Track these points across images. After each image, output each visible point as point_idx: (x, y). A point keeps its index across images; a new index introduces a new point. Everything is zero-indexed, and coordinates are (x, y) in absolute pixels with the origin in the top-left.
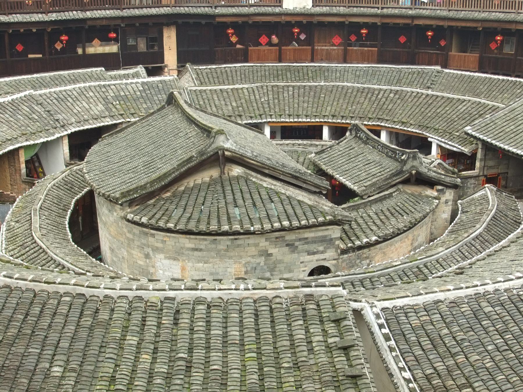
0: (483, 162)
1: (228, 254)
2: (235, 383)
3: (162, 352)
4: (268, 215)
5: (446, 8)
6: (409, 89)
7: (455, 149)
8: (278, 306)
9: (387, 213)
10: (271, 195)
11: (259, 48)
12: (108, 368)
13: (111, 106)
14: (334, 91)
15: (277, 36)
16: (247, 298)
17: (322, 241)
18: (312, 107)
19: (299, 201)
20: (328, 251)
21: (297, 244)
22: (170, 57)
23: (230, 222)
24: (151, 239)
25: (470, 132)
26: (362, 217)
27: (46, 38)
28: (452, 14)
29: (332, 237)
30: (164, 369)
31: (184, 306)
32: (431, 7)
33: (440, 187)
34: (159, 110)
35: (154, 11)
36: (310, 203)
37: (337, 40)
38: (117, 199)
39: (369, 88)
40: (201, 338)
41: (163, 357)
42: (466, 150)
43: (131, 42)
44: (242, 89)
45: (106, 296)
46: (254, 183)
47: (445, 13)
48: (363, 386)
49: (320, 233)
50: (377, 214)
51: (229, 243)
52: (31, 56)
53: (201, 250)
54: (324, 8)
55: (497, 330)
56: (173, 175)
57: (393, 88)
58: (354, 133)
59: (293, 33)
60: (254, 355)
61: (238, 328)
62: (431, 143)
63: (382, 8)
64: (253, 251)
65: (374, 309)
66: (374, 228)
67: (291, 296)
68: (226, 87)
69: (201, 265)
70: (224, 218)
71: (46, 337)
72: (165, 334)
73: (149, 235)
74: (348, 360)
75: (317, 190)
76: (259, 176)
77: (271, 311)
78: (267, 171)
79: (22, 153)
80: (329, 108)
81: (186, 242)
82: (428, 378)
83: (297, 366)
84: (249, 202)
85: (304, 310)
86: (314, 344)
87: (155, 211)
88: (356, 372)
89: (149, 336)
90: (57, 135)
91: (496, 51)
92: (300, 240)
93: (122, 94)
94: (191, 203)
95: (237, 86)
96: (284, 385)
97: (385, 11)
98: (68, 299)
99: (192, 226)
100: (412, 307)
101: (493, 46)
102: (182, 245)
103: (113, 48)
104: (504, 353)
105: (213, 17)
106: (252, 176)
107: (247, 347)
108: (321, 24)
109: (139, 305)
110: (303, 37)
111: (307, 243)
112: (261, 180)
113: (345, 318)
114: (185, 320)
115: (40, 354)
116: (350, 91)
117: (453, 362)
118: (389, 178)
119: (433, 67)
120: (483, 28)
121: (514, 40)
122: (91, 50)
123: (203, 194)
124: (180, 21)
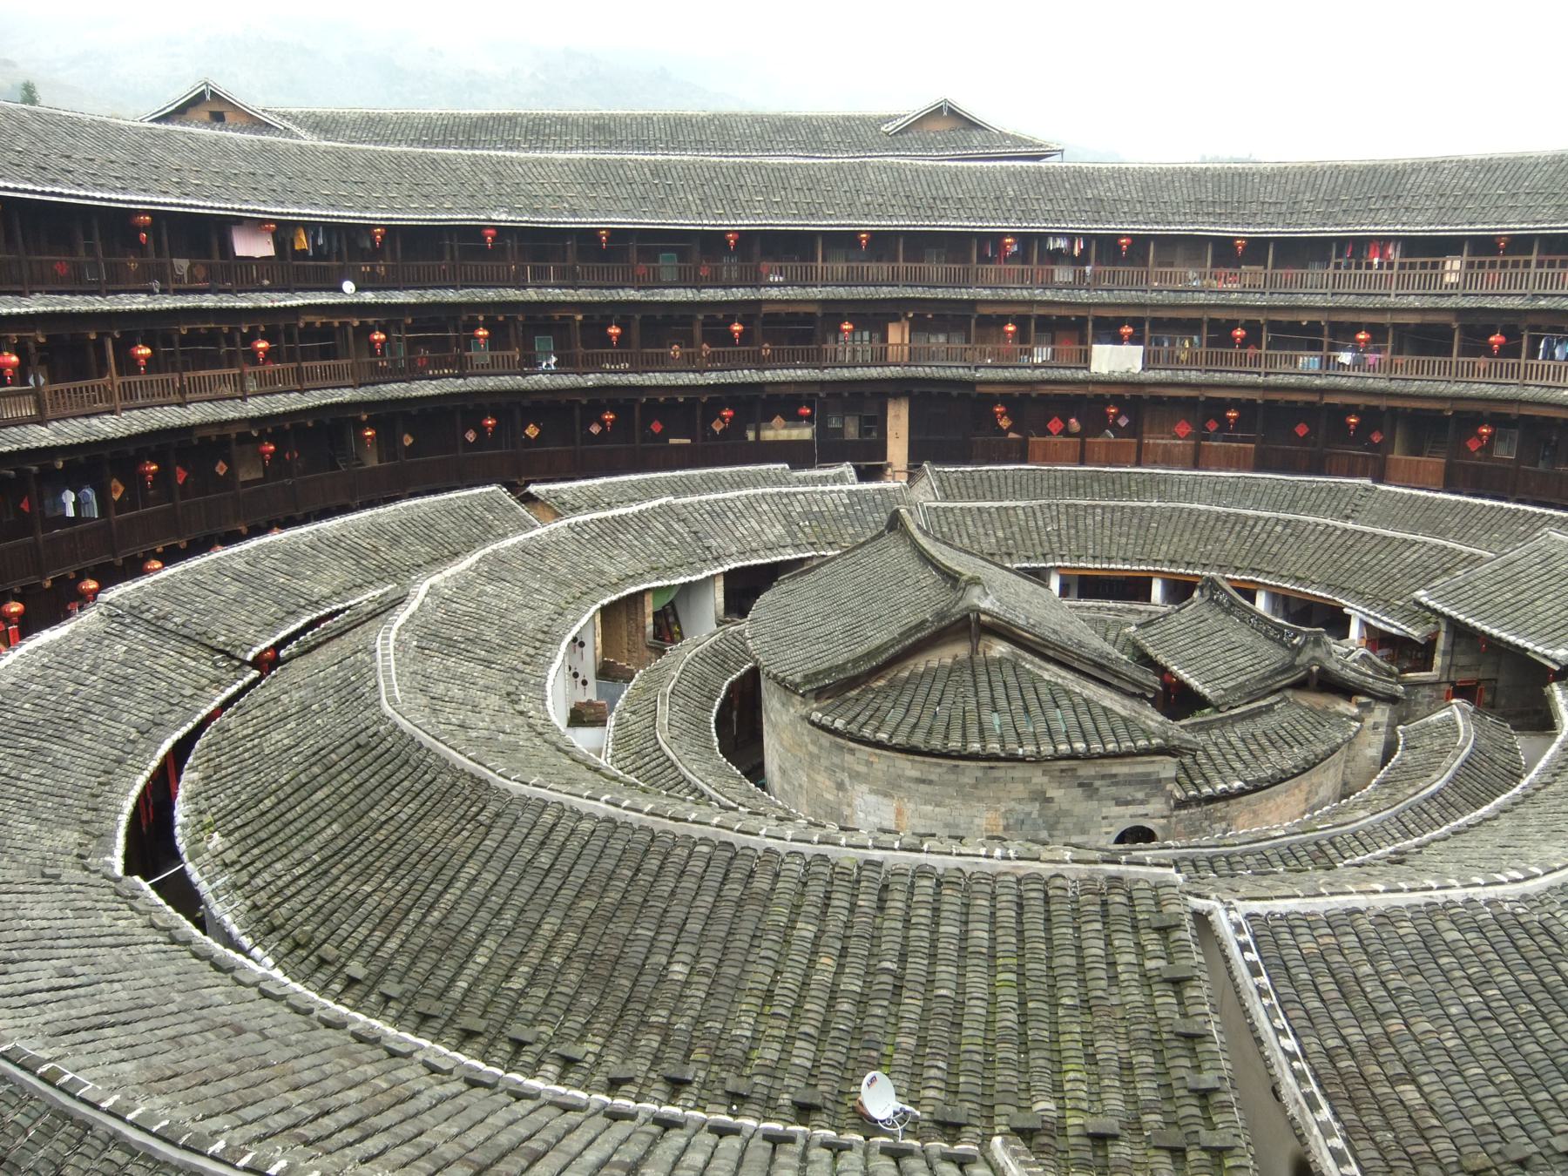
0: (1448, 658)
1: (977, 793)
2: (975, 1025)
3: (855, 955)
4: (1049, 729)
6: (1311, 519)
7: (1394, 631)
8: (1060, 892)
9: (1264, 741)
10: (1057, 695)
11: (1047, 439)
12: (761, 975)
13: (795, 528)
14: (1174, 519)
15: (1078, 419)
16: (1006, 874)
17: (1143, 782)
18: (1135, 545)
19: (1104, 708)
20: (1153, 800)
21: (1097, 783)
22: (897, 450)
23: (983, 739)
24: (848, 757)
25: (1424, 600)
26: (1216, 744)
27: (699, 413)
28: (1394, 386)
29: (1162, 776)
30: (856, 986)
31: (896, 878)
33: (1363, 699)
34: (873, 539)
35: (874, 372)
36: (1124, 713)
37: (1183, 428)
38: (797, 686)
39: (1238, 515)
40: (921, 938)
41: (854, 966)
42: (1416, 633)
43: (834, 423)
44: (1014, 508)
45: (768, 850)
46: (1029, 672)
47: (1382, 384)
48: (1207, 1056)
49: (1140, 767)
50: (1243, 740)
51: (979, 774)
52: (672, 441)
53: (930, 782)
54: (1163, 373)
55: (1469, 978)
56: (892, 651)
57: (1282, 515)
58: (1207, 593)
59: (1107, 415)
60: (1013, 977)
61: (986, 926)
62: (1347, 619)
63: (1267, 374)
64: (1019, 790)
65: (1233, 915)
66: (1238, 765)
67: (1083, 876)
68: (987, 504)
69: (930, 808)
70: (973, 730)
71: (665, 911)
72: (861, 923)
74: (1180, 1003)
75: (1138, 691)
76: (1037, 660)
77: (1047, 900)
78: (1050, 653)
79: (649, 599)
80: (1164, 548)
81: (908, 767)
82: (1330, 1055)
83: (1086, 1005)
84: (1017, 704)
85: (1104, 903)
86: (1120, 968)
87: (857, 709)
88: (1194, 1029)
89: (834, 926)
90: (707, 573)
92: (1103, 777)
93: (815, 509)
94: (919, 699)
95: (1006, 503)
96: (1062, 1038)
97: (1271, 378)
98: (705, 849)
99: (918, 740)
100: (1304, 917)
101: (1473, 445)
103: (805, 433)
104: (1481, 1025)
105: (972, 384)
107: (1000, 961)
108: (1157, 401)
109: (821, 869)
110: (1123, 422)
111: (1116, 784)
112: (1040, 667)
113: (1178, 926)
114: (896, 903)
115: (654, 939)
116: (1203, 518)
117: (1379, 1030)
118: (1269, 677)
119: (1356, 481)
120: (1456, 412)
121: (1516, 434)
122: (768, 435)
123: (939, 686)
124: (916, 390)
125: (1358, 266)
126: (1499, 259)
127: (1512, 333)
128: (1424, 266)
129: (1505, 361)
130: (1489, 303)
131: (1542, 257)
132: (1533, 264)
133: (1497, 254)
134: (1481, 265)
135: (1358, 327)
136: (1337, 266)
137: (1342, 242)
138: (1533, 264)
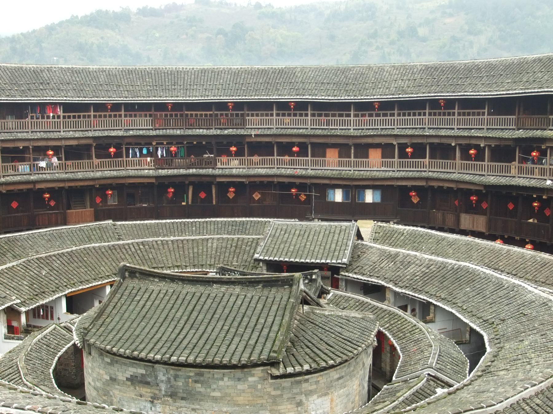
1: (355, 372)
5: (63, 171)
32: (49, 171)
69: (342, 390)
73: (302, 382)
81: (334, 374)
91: (101, 204)
102: (331, 379)
106: (315, 309)
121: (116, 192)
125: (43, 118)
126: (107, 114)
127: (118, 147)
128: (84, 117)
129: (117, 159)
130: (106, 134)
131: (126, 113)
132: (123, 116)
133: (108, 112)
134: (100, 116)
135: (47, 148)
136: (32, 118)
137: (33, 106)
138: (123, 116)
